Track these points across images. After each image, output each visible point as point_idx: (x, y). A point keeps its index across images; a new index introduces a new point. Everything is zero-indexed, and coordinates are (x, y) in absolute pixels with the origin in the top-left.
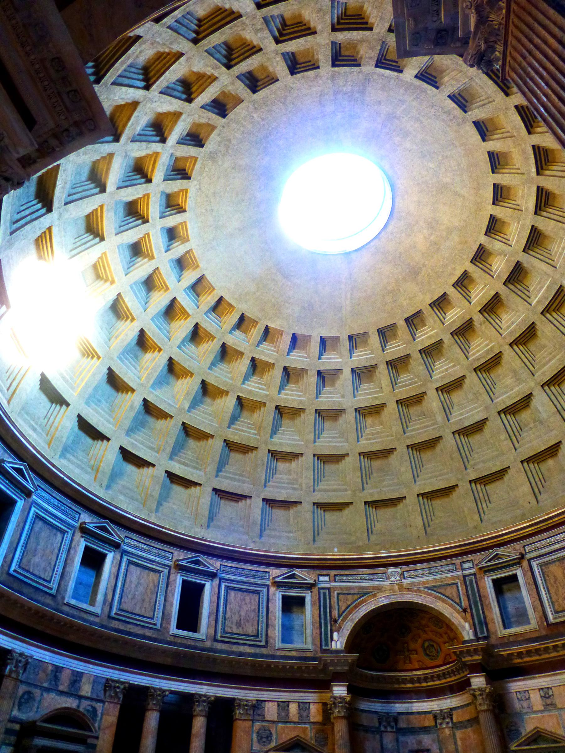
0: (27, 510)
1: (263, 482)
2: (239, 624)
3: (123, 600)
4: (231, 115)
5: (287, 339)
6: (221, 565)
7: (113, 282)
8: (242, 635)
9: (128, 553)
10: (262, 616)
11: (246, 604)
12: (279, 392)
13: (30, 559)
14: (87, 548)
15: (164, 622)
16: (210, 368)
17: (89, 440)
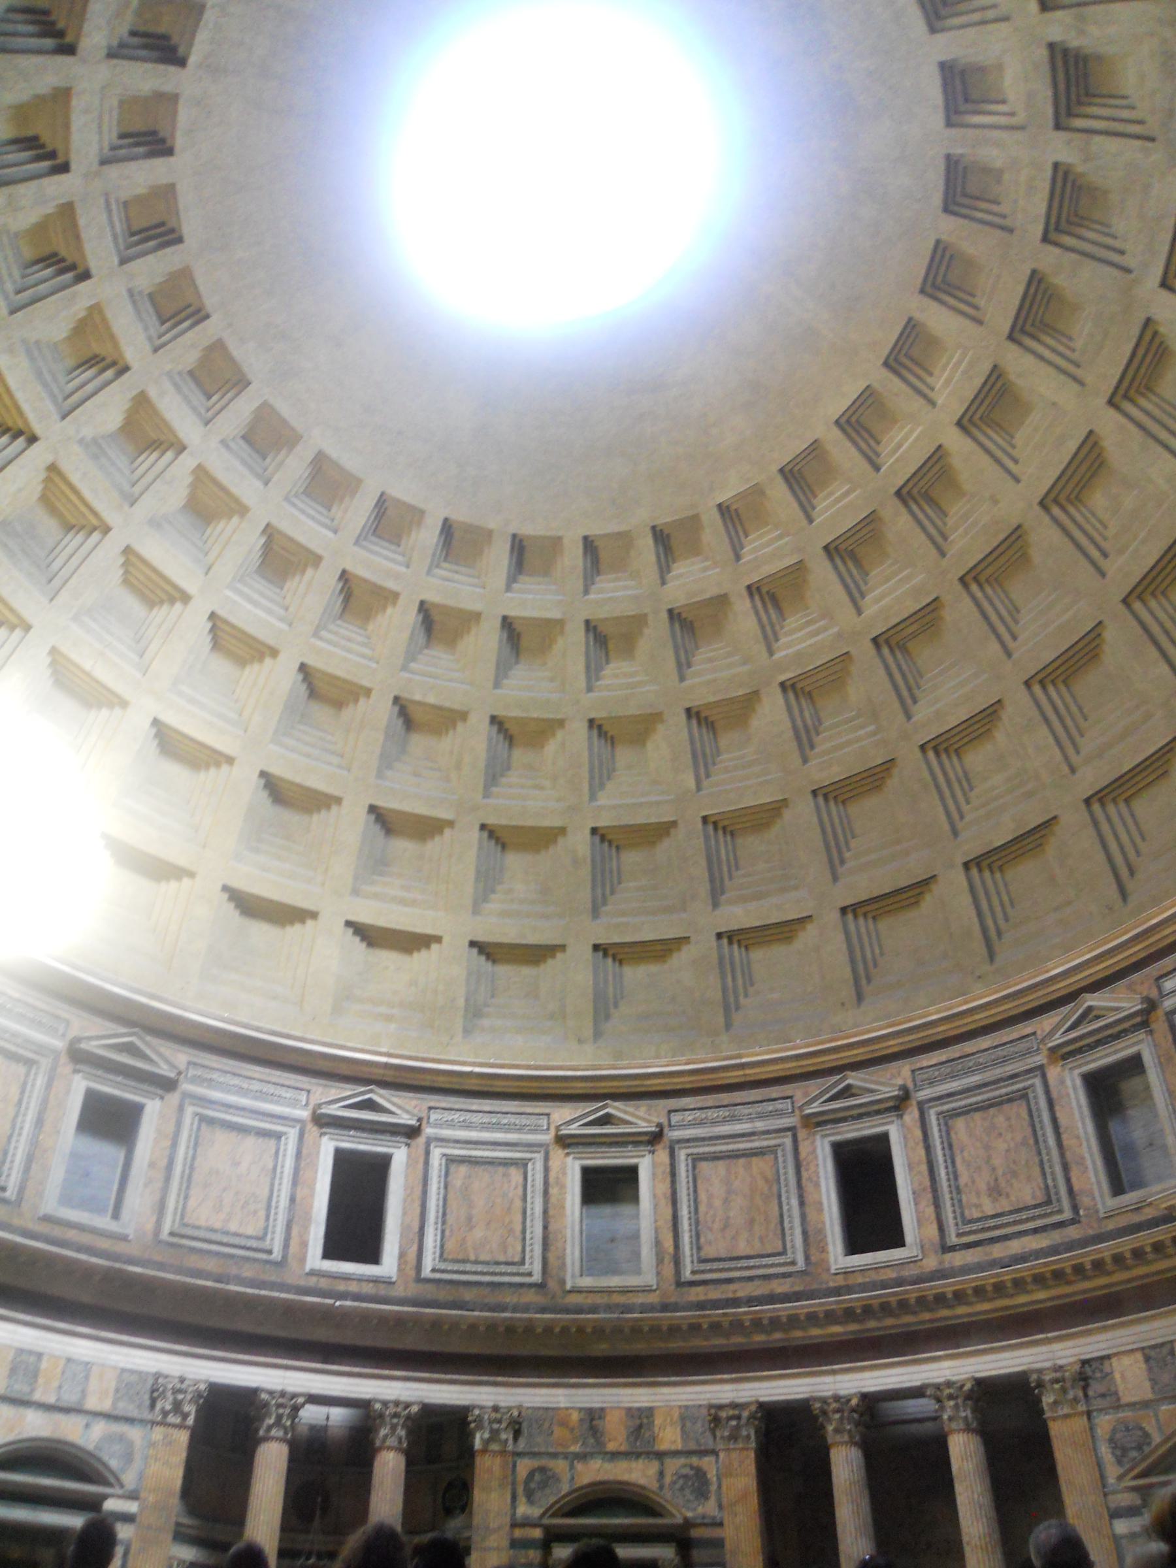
0: (422, 1160)
1: (946, 827)
2: (995, 1191)
3: (702, 1240)
4: (210, 302)
5: (779, 492)
6: (913, 1071)
7: (368, 692)
8: (1011, 1212)
9: (688, 1141)
10: (1047, 1148)
11: (1000, 1134)
12: (859, 612)
13: (464, 1239)
14: (587, 1172)
15: (813, 1251)
16: (682, 678)
17: (527, 971)
